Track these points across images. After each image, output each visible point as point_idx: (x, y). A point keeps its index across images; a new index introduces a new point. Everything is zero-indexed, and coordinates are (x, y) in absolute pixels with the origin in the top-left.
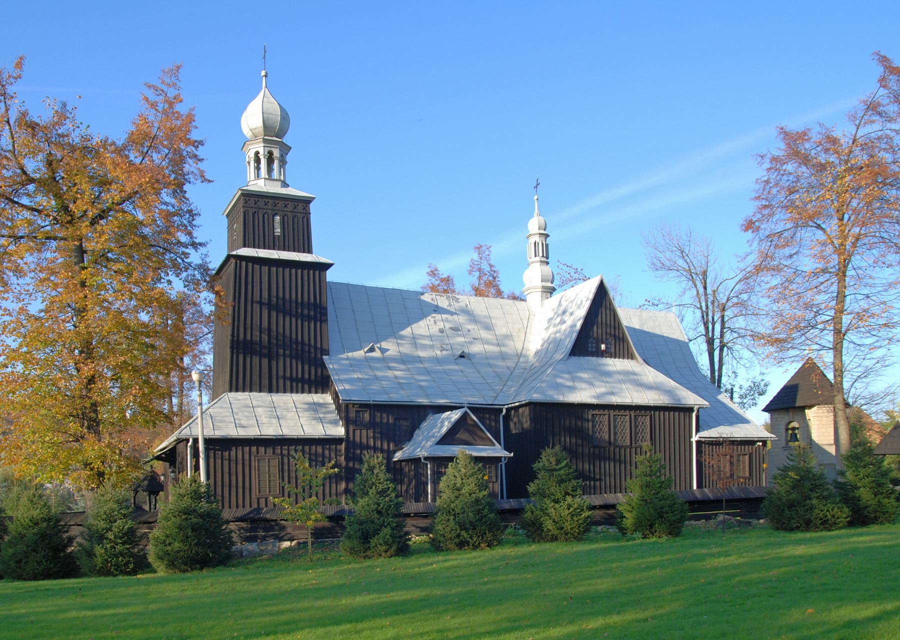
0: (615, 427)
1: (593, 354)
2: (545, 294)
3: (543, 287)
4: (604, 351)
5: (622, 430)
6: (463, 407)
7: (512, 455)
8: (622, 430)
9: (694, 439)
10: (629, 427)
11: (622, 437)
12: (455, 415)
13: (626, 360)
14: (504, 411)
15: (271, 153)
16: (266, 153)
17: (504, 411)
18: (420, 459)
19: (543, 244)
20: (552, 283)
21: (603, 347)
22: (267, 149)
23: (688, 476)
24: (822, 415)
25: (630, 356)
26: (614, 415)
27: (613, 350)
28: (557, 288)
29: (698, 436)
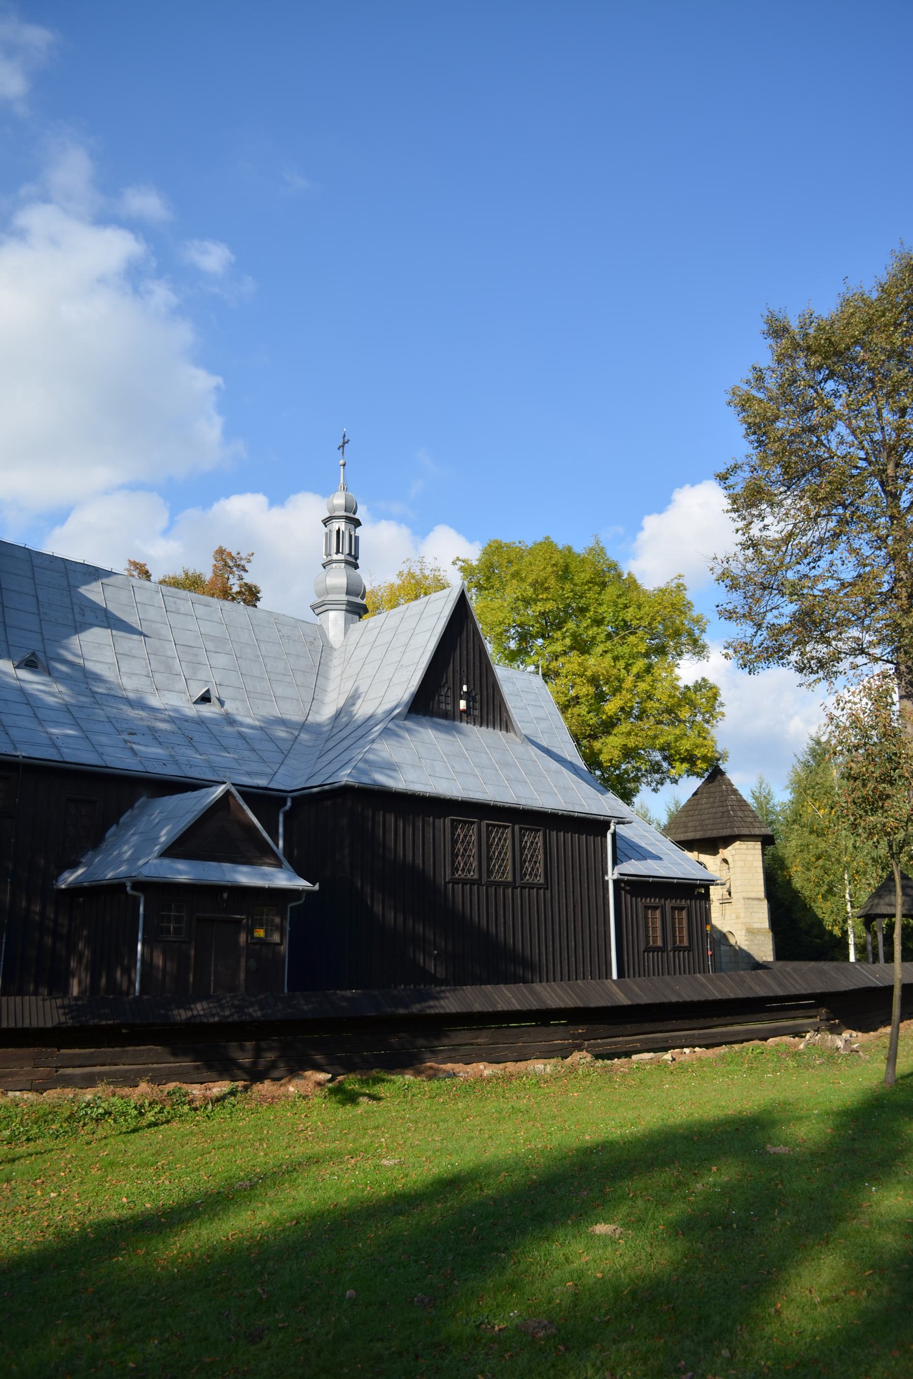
0: (489, 846)
1: (445, 716)
2: (350, 616)
3: (349, 603)
4: (463, 711)
5: (500, 853)
6: (224, 783)
7: (317, 887)
8: (500, 853)
9: (611, 875)
10: (510, 848)
11: (500, 866)
12: (220, 790)
13: (497, 731)
14: (289, 804)
17: (289, 804)
18: (122, 886)
19: (350, 536)
20: (363, 598)
21: (463, 704)
23: (602, 943)
24: (746, 852)
25: (504, 726)
26: (488, 825)
27: (477, 713)
28: (370, 608)
29: (616, 871)
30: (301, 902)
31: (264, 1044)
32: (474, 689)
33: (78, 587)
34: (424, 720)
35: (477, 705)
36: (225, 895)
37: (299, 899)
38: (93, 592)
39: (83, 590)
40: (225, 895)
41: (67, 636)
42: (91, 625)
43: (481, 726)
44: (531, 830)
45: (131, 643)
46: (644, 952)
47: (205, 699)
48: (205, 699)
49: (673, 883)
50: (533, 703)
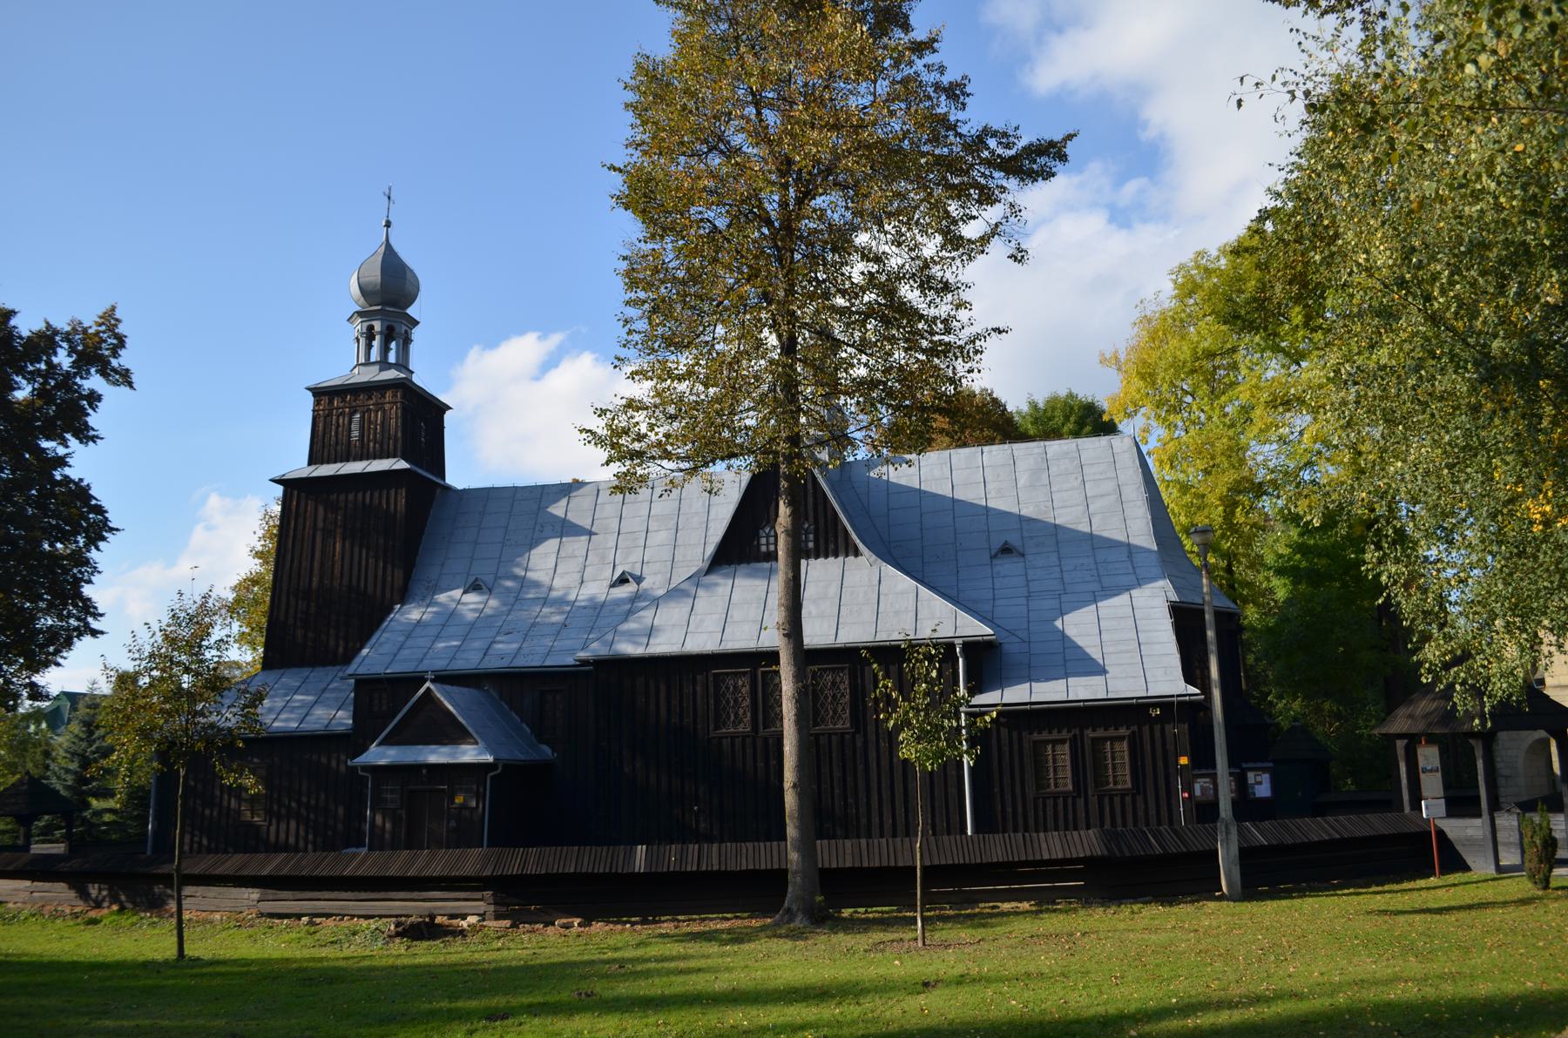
15: (371, 328)
16: (364, 330)
22: (366, 324)
27: (811, 545)
30: (499, 771)
31: (102, 886)
32: (807, 519)
33: (547, 507)
34: (743, 568)
35: (811, 536)
36: (424, 771)
37: (497, 769)
38: (558, 510)
39: (549, 510)
40: (424, 771)
41: (521, 555)
42: (546, 539)
43: (847, 556)
44: (833, 670)
45: (576, 545)
46: (1036, 799)
47: (623, 580)
48: (623, 580)
49: (1132, 705)
50: (1098, 477)
